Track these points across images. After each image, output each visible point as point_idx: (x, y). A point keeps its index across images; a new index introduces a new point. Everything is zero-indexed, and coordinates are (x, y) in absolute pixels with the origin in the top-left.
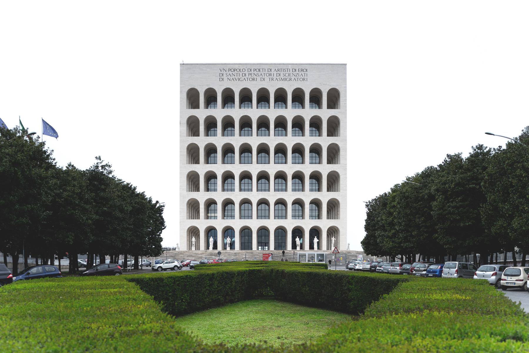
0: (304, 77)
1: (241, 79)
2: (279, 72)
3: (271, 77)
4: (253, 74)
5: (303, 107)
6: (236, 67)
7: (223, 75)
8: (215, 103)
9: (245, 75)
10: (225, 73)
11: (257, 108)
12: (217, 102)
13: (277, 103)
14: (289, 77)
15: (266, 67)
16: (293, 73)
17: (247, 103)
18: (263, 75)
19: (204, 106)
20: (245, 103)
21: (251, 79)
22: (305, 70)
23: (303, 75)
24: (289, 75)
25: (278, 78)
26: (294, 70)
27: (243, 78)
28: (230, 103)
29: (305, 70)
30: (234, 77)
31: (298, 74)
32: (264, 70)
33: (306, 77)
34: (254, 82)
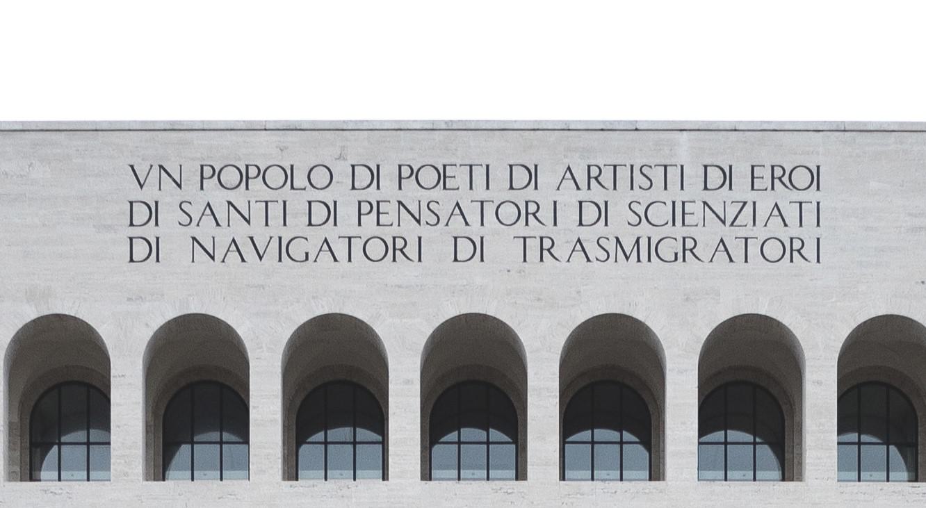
0: (794, 230)
1: (297, 250)
2: (597, 194)
3: (534, 229)
4: (390, 209)
5: (789, 468)
6: (262, 151)
7: (154, 212)
8: (95, 435)
9: (332, 212)
10: (169, 197)
11: (427, 475)
12: (107, 427)
13: (585, 435)
14: (679, 231)
15: (498, 154)
16: (709, 197)
17: (344, 433)
18: (474, 218)
19: (10, 461)
20: (334, 434)
21: (376, 249)
22: (802, 178)
23: (791, 213)
24: (679, 214)
25: (588, 235)
26: (715, 177)
27: (317, 236)
28: (215, 436)
29: (802, 178)
30: (240, 230)
31: (748, 209)
32: (479, 174)
33: (809, 233)
34: (403, 271)
